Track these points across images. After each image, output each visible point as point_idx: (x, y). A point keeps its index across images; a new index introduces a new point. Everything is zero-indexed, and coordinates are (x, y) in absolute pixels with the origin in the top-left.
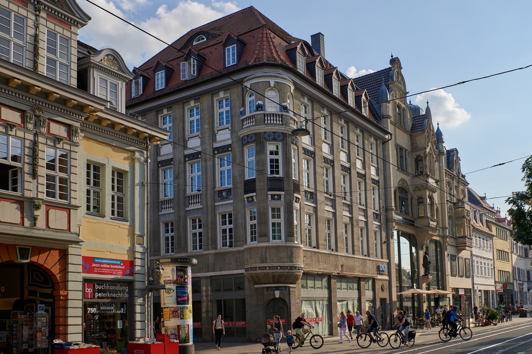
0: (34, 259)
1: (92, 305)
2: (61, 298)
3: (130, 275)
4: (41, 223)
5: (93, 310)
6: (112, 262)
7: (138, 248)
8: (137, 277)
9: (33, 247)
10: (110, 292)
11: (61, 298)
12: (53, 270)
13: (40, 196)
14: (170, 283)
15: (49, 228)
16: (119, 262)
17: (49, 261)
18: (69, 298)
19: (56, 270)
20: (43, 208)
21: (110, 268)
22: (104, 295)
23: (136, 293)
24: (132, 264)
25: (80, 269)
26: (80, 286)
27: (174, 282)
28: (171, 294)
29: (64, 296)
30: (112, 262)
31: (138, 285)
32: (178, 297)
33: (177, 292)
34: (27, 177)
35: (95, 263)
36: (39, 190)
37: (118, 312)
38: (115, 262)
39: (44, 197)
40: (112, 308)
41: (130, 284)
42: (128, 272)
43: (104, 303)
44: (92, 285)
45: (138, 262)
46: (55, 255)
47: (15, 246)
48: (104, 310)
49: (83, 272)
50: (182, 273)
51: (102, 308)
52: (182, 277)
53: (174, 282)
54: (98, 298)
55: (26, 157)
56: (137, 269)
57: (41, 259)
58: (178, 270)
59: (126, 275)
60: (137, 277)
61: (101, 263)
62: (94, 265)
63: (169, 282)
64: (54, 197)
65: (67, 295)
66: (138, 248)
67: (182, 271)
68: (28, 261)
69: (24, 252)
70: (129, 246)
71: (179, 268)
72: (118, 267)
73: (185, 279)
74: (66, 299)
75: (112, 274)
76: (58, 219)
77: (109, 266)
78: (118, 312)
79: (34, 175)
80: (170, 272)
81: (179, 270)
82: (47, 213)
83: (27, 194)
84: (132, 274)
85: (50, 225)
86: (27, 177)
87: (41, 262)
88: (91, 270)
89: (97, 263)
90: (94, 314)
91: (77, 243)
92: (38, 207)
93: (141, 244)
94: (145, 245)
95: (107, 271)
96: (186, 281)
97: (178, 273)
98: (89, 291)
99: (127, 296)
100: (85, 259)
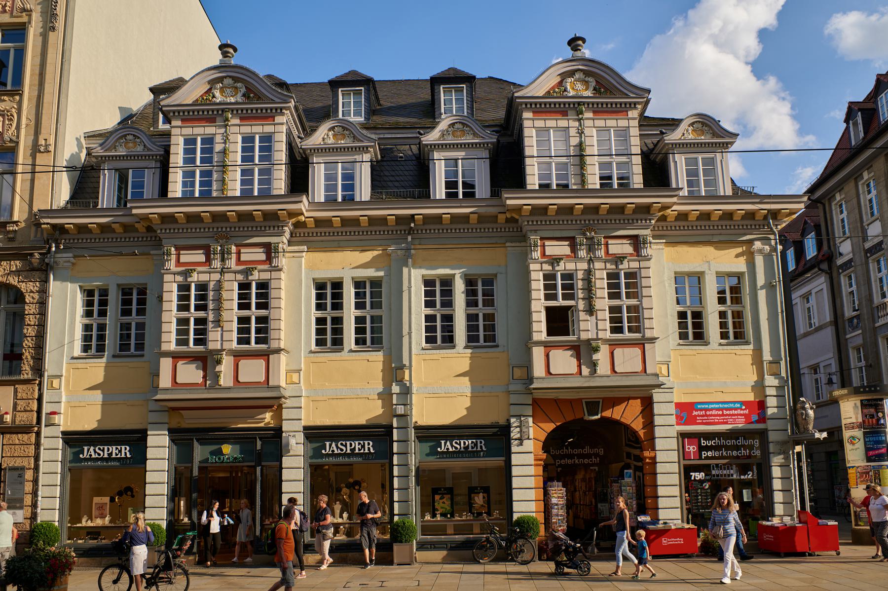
0: (607, 414)
1: (698, 468)
2: (647, 460)
3: (758, 422)
4: (603, 368)
5: (700, 476)
6: (726, 406)
7: (771, 381)
8: (770, 425)
9: (604, 399)
10: (727, 448)
11: (647, 460)
12: (633, 426)
13: (601, 335)
14: (853, 428)
15: (616, 372)
16: (738, 405)
17: (629, 414)
18: (658, 460)
19: (638, 425)
20: (604, 350)
21: (723, 415)
22: (717, 454)
23: (772, 448)
24: (761, 405)
25: (673, 420)
26: (673, 444)
27: (861, 426)
28: (857, 446)
29: (650, 458)
30: (726, 406)
31: (772, 436)
32: (867, 450)
33: (865, 442)
34: (583, 316)
35: (697, 410)
36: (599, 328)
37: (742, 477)
38: (732, 405)
39: (608, 335)
40: (732, 472)
41: (762, 435)
42: (755, 418)
43: (717, 465)
44: (696, 440)
45: (772, 402)
46: (636, 406)
47: (581, 400)
48: (718, 476)
49: (678, 424)
50: (872, 410)
51: (713, 472)
52: (872, 416)
53: (861, 426)
54: (707, 458)
55: (580, 291)
56: (770, 411)
57: (616, 413)
58: (864, 405)
59: (752, 423)
60: (770, 425)
61: (706, 410)
62: (695, 413)
63: (851, 426)
64: (622, 333)
65: (655, 457)
66: (771, 381)
67: (870, 406)
68: (599, 416)
69: (593, 407)
70: (756, 379)
71: (865, 402)
72: (736, 412)
73: (879, 420)
74: (654, 462)
75: (726, 423)
76: (628, 360)
77: (720, 413)
78: (742, 477)
79: (591, 310)
80: (852, 410)
81: (866, 405)
82: (612, 354)
83: (584, 336)
84: (763, 419)
85: (617, 369)
86: (583, 316)
87: (616, 416)
88: (692, 421)
89: (701, 410)
90: (701, 482)
91: (659, 386)
92: (596, 350)
93: (777, 375)
94: (783, 374)
95: (716, 419)
96: (882, 421)
97: (865, 411)
98: (692, 449)
99: (758, 453)
100: (678, 405)
